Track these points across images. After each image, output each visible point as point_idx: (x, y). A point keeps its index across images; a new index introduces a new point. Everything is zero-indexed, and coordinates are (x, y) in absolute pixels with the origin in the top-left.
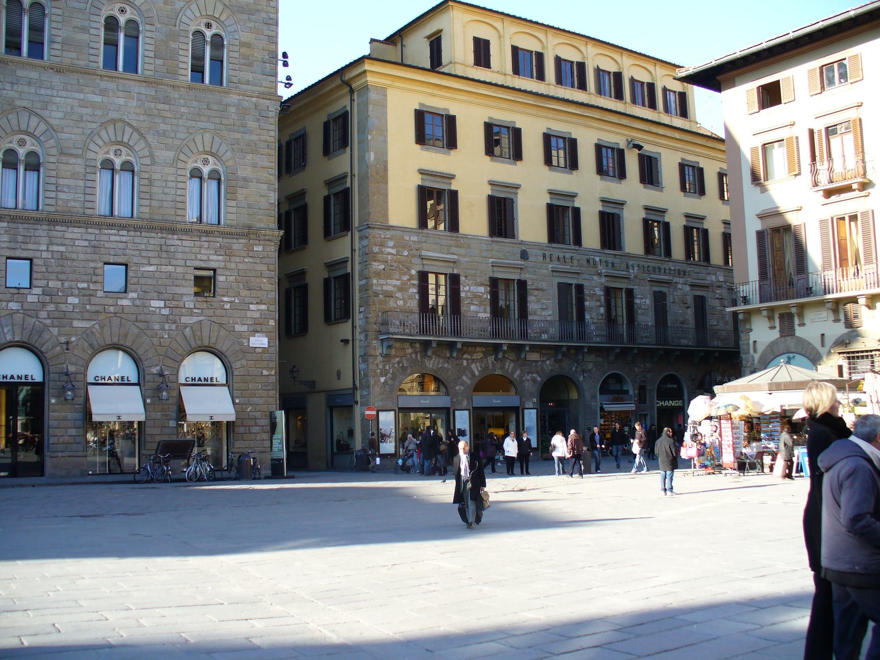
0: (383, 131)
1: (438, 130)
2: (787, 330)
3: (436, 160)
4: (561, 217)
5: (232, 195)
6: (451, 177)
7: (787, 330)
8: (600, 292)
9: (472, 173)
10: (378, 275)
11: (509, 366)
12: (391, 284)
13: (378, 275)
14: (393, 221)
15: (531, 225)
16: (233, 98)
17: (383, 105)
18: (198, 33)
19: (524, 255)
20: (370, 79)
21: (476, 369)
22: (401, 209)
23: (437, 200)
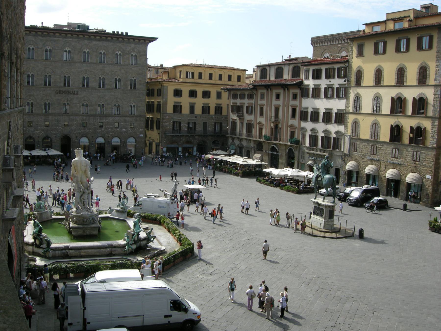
0: (167, 95)
1: (178, 93)
2: (233, 141)
3: (178, 99)
4: (205, 109)
5: (137, 110)
6: (181, 102)
7: (233, 141)
8: (213, 124)
9: (185, 101)
10: (164, 122)
11: (191, 139)
12: (167, 124)
13: (164, 122)
14: (168, 112)
15: (198, 111)
16: (138, 91)
17: (167, 89)
18: (132, 79)
19: (196, 117)
20: (165, 85)
21: (184, 139)
22: (170, 109)
23: (177, 108)
